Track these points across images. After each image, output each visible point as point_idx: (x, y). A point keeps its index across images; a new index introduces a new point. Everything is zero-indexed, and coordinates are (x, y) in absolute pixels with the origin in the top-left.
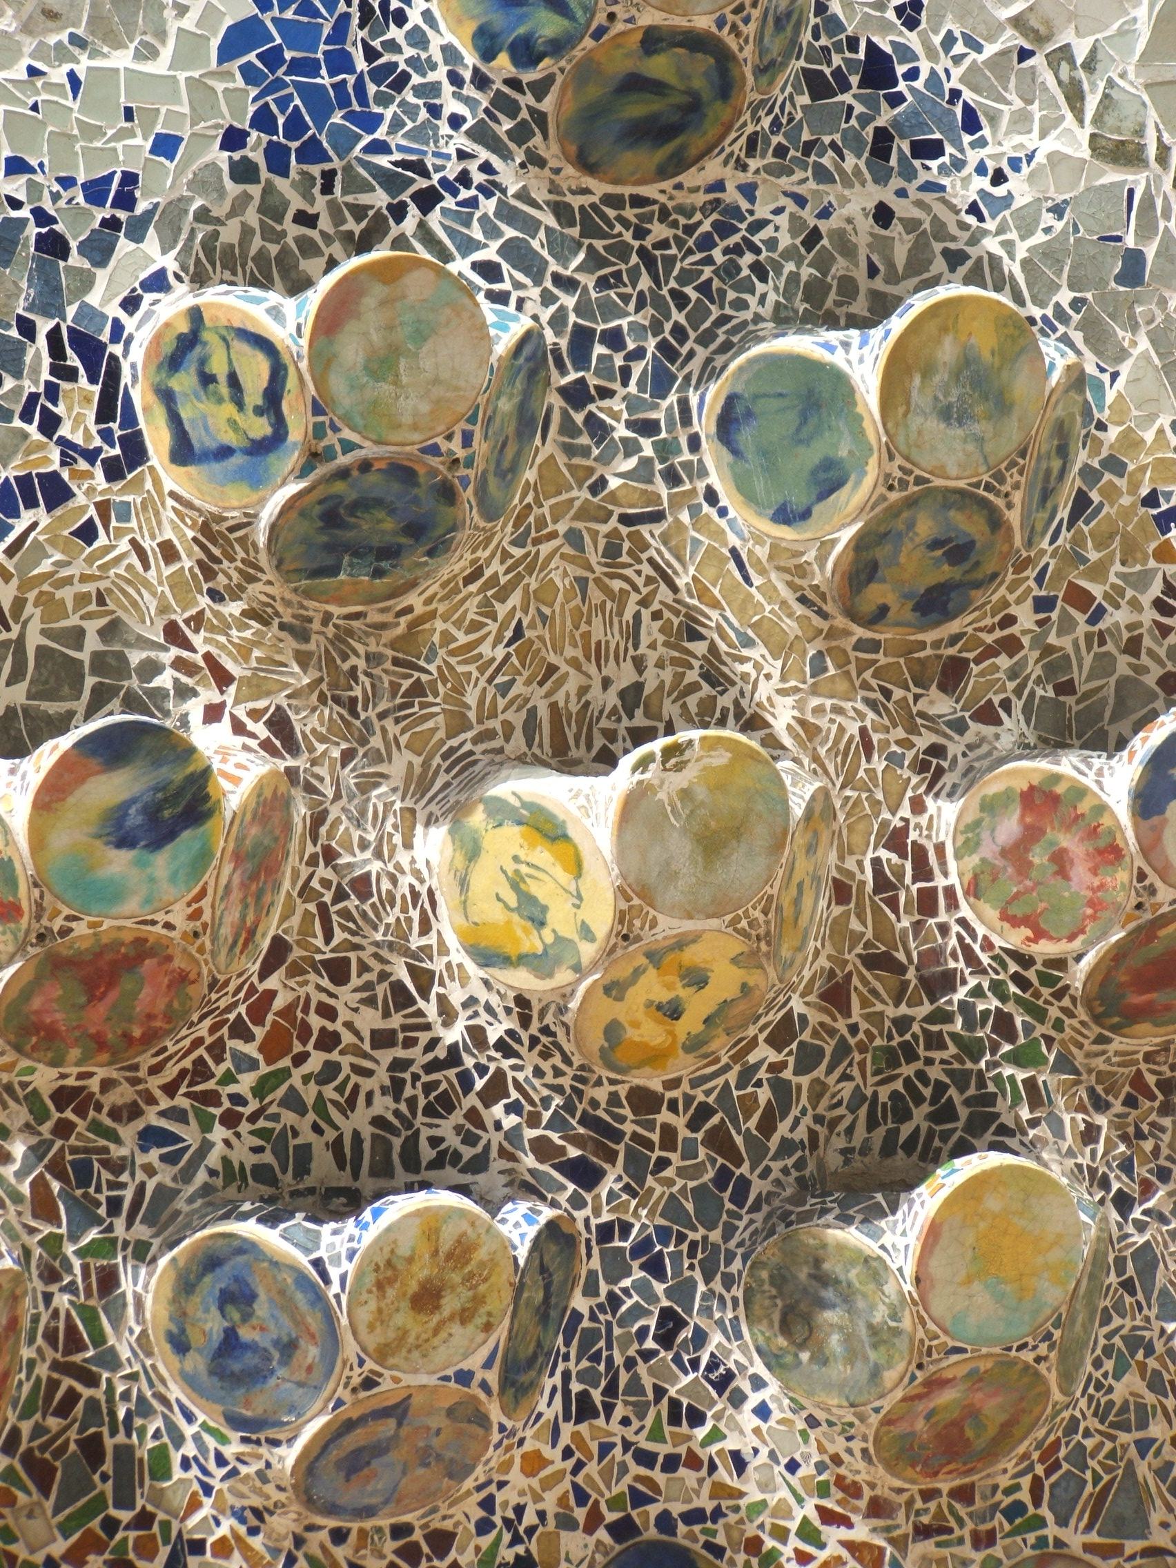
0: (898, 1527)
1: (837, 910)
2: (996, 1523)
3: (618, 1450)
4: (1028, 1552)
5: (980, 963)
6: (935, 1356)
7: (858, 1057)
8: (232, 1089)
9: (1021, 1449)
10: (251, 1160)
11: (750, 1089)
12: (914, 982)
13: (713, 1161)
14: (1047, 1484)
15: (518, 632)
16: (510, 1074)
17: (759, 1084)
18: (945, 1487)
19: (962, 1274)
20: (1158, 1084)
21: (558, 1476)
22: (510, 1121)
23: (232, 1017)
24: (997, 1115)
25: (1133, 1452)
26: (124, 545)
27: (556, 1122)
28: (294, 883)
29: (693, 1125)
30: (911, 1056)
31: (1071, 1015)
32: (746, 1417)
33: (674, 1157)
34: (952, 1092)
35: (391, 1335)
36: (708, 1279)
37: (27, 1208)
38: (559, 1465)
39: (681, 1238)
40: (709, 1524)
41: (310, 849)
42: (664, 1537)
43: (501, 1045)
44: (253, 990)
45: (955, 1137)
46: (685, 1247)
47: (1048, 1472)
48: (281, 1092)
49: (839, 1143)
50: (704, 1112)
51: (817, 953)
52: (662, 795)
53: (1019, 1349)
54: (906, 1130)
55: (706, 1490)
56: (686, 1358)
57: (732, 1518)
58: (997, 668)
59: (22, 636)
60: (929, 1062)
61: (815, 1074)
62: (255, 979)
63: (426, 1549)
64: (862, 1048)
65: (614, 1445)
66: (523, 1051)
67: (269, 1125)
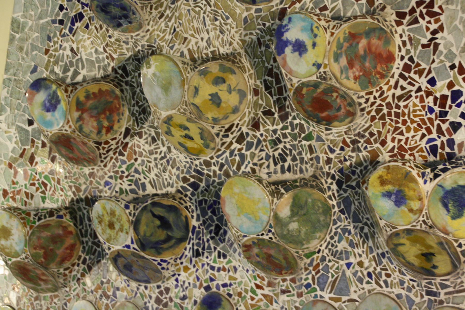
0: (276, 290)
1: (255, 98)
2: (303, 290)
3: (206, 266)
4: (312, 299)
7: (264, 144)
8: (121, 169)
10: (128, 188)
15: (175, 30)
17: (236, 155)
18: (288, 278)
19: (236, 213)
20: (351, 142)
23: (118, 150)
25: (345, 267)
26: (93, 27)
27: (188, 172)
28: (129, 112)
29: (220, 170)
30: (280, 142)
35: (108, 236)
37: (84, 203)
41: (133, 102)
42: (217, 291)
44: (122, 143)
47: (317, 273)
48: (133, 169)
49: (266, 171)
50: (222, 165)
51: (250, 113)
52: (149, 76)
54: (286, 165)
55: (227, 278)
57: (234, 286)
58: (295, 8)
59: (81, 57)
60: (285, 143)
62: (122, 139)
63: (164, 292)
64: (265, 140)
67: (132, 178)
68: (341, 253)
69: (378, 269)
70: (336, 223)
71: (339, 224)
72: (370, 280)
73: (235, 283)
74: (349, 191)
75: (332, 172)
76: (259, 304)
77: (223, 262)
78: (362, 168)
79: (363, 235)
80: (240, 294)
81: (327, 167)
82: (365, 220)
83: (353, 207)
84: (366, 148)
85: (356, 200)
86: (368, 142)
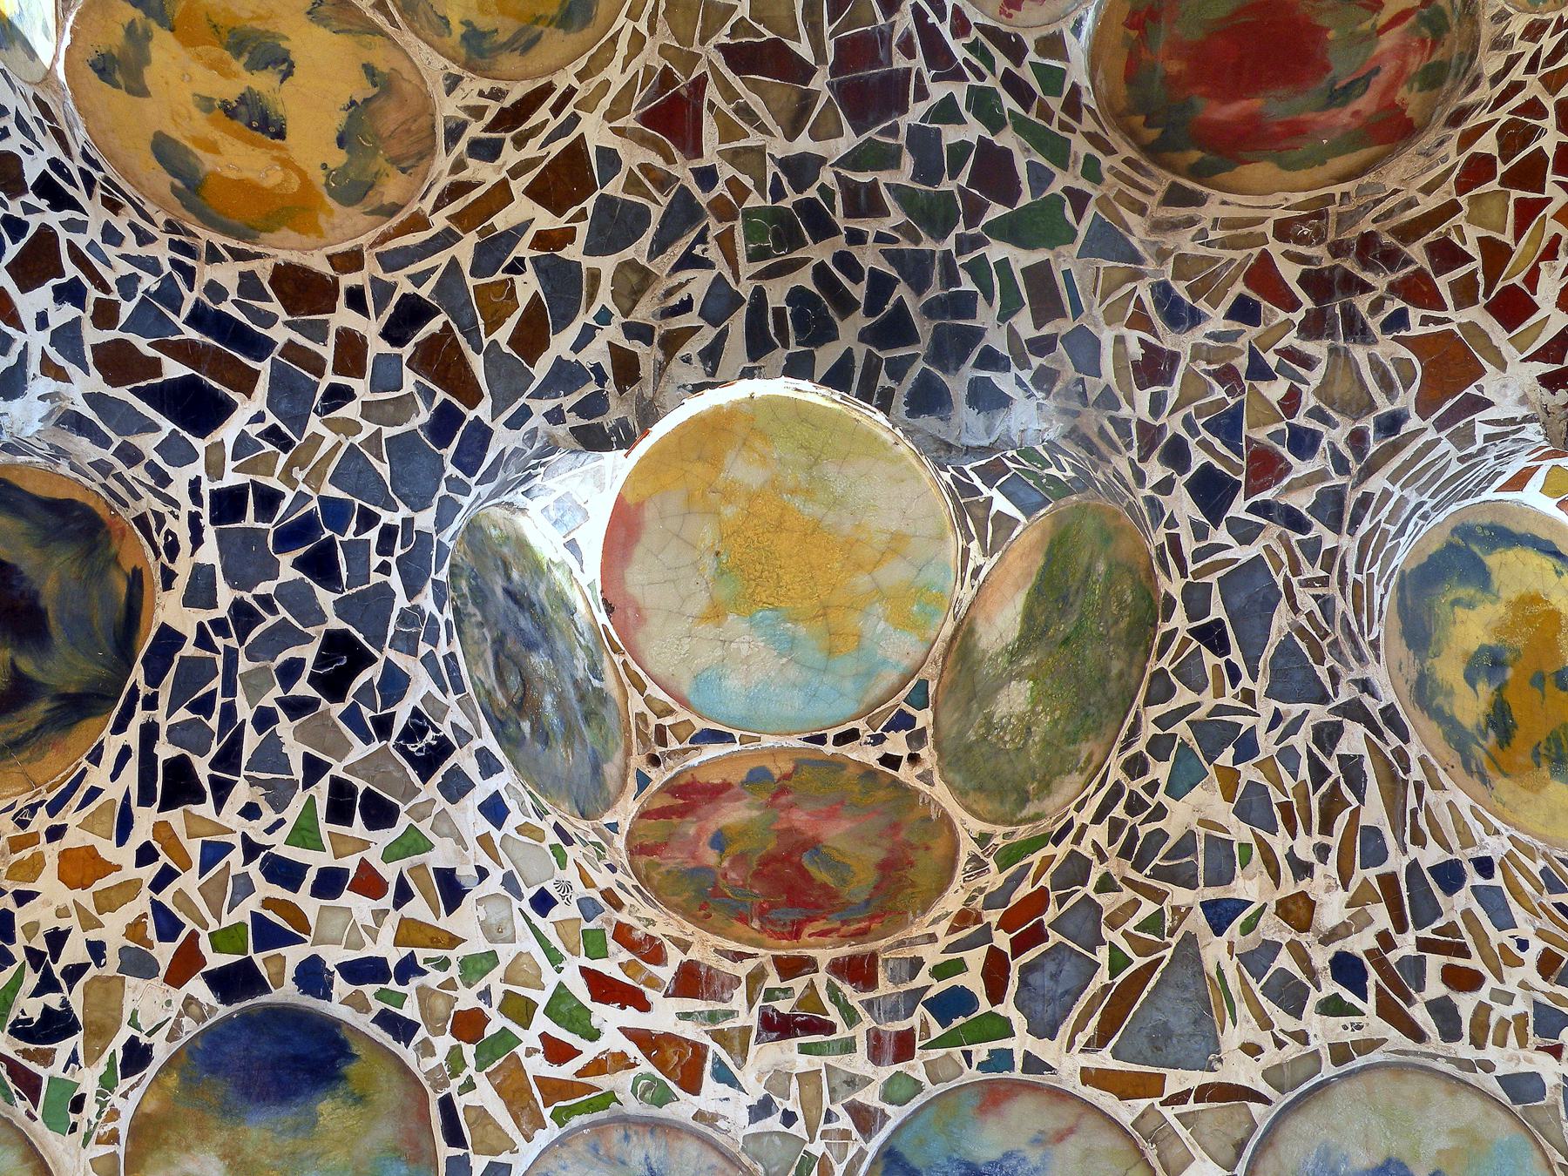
0: (730, 1014)
2: (914, 1021)
3: (236, 857)
4: (972, 1075)
5: (952, 58)
6: (674, 745)
7: (716, 228)
9: (952, 901)
11: (500, 276)
12: (826, 94)
13: (429, 396)
14: (1015, 966)
16: (63, 236)
17: (517, 267)
18: (824, 956)
19: (700, 603)
20: (1304, 281)
21: (129, 890)
22: (63, 314)
24: (979, 333)
25: (1198, 921)
27: (148, 319)
29: (395, 333)
30: (823, 228)
31: (1109, 151)
32: (468, 816)
33: (361, 386)
34: (902, 291)
36: (412, 592)
38: (130, 871)
39: (368, 520)
40: (392, 985)
43: (44, 186)
45: (914, 373)
46: (373, 535)
47: (1019, 946)
50: (411, 314)
51: (637, 41)
53: (841, 739)
55: (388, 932)
56: (367, 713)
57: (434, 978)
60: (856, 237)
61: (628, 253)
64: (723, 210)
65: (230, 847)
66: (80, 195)
68: (1186, 845)
69: (1407, 945)
70: (1170, 692)
71: (1184, 696)
72: (1349, 997)
73: (443, 964)
74: (1272, 532)
75: (1174, 425)
76: (603, 1082)
77: (365, 845)
78: (1368, 423)
79: (1332, 765)
80: (468, 1025)
81: (1143, 397)
82: (1346, 694)
83: (1281, 620)
84: (1397, 321)
85: (1308, 583)
86: (1418, 291)
